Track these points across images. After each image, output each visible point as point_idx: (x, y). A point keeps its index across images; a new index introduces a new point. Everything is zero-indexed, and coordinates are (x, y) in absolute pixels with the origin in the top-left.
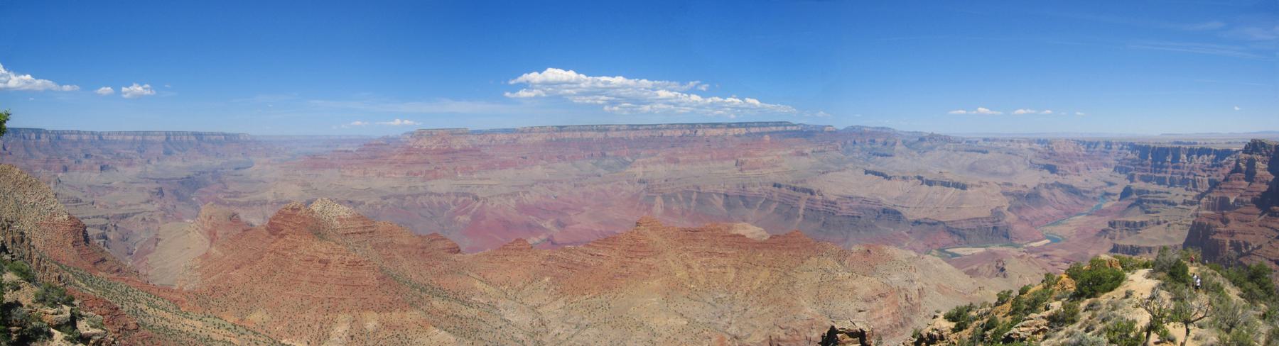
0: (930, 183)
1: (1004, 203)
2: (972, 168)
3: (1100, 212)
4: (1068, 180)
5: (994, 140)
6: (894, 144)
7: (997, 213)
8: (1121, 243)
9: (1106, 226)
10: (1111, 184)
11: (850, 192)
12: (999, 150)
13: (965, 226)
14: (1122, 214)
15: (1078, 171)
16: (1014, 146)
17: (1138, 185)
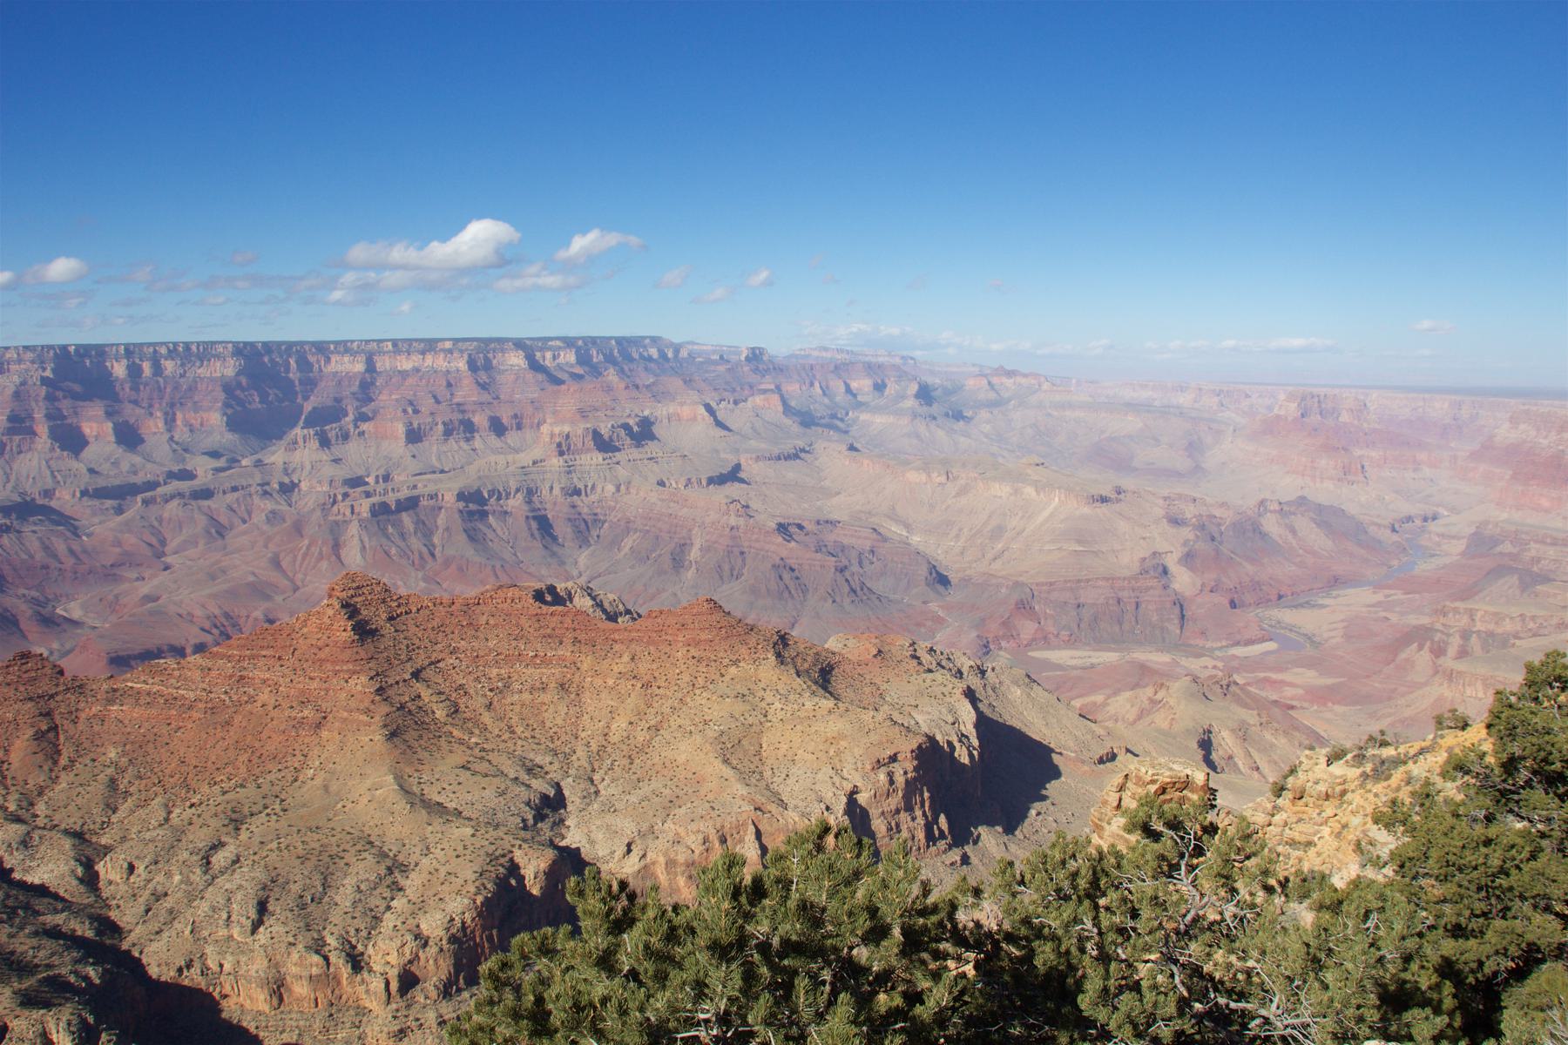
1: (1170, 544)
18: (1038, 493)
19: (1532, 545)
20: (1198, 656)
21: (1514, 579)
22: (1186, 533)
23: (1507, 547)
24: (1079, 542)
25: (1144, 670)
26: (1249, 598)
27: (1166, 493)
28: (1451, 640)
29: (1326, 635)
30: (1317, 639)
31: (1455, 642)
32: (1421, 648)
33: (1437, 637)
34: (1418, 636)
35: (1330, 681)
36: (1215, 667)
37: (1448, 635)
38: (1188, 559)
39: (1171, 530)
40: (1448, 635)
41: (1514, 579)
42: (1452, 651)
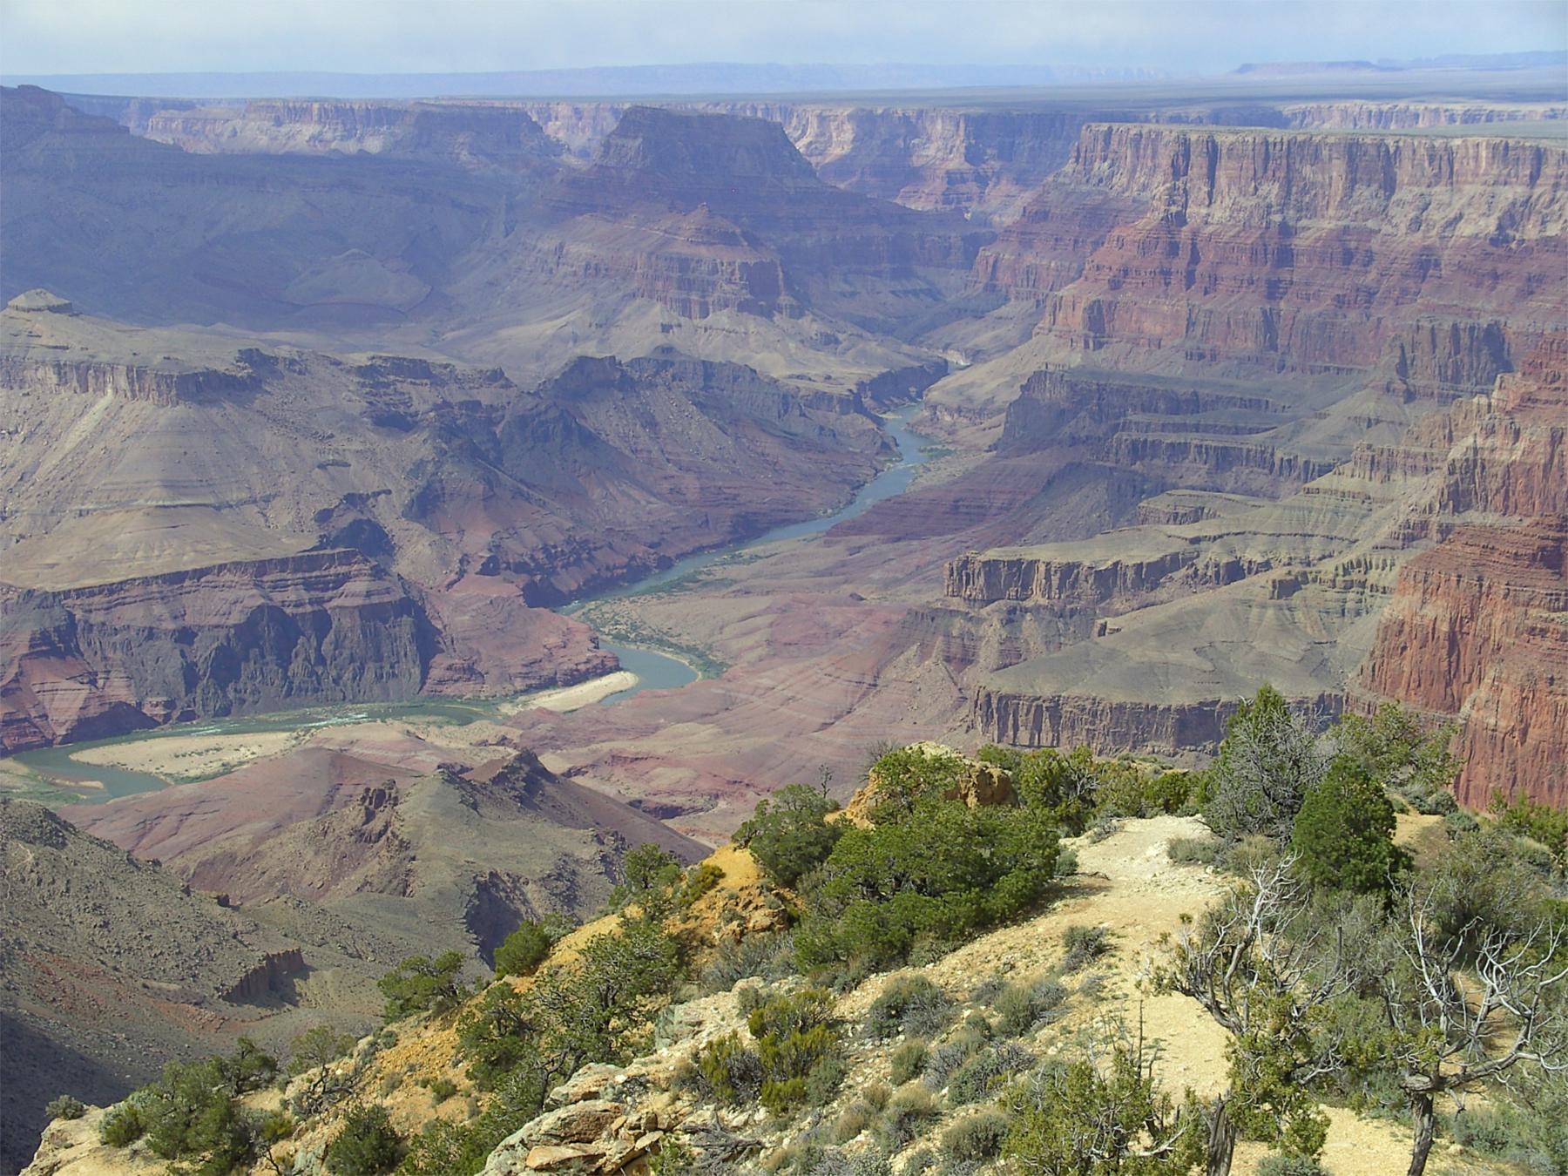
8: (1003, 684)
9: (934, 596)
18: (63, 380)
19: (1133, 417)
20: (465, 720)
22: (418, 446)
23: (1083, 425)
24: (171, 486)
25: (340, 761)
26: (568, 581)
27: (362, 359)
28: (984, 629)
29: (735, 645)
30: (717, 657)
32: (923, 655)
33: (958, 625)
35: (748, 744)
36: (503, 741)
37: (979, 621)
38: (425, 506)
39: (383, 443)
40: (979, 621)
42: (987, 654)
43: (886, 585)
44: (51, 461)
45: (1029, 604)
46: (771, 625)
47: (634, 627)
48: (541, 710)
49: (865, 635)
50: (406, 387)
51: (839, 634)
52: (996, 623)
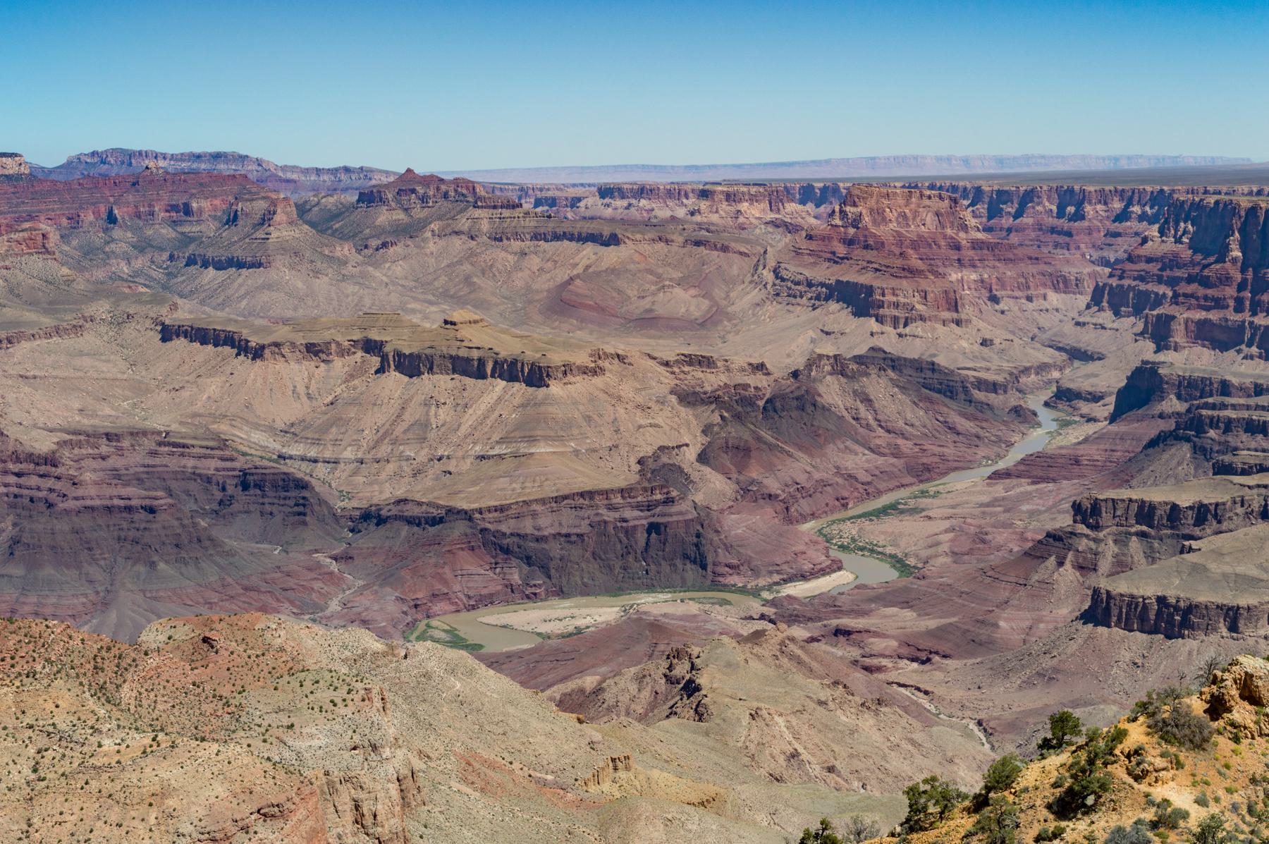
0: (411, 365)
1: (684, 432)
2: (563, 303)
3: (1039, 468)
4: (916, 343)
5: (642, 191)
6: (266, 219)
7: (660, 473)
9: (1064, 521)
10: (1079, 355)
11: (107, 415)
12: (660, 231)
13: (547, 523)
14: (1124, 473)
15: (954, 306)
16: (716, 215)
17: (1188, 359)
21: (1185, 450)
29: (924, 554)
31: (1110, 549)
32: (1061, 564)
34: (1056, 541)
35: (932, 623)
39: (685, 412)
41: (1185, 450)
42: (1105, 565)
43: (1031, 514)
44: (469, 420)
45: (1133, 530)
46: (951, 541)
47: (853, 540)
48: (788, 596)
49: (1016, 549)
50: (700, 375)
51: (999, 548)
52: (1111, 542)
